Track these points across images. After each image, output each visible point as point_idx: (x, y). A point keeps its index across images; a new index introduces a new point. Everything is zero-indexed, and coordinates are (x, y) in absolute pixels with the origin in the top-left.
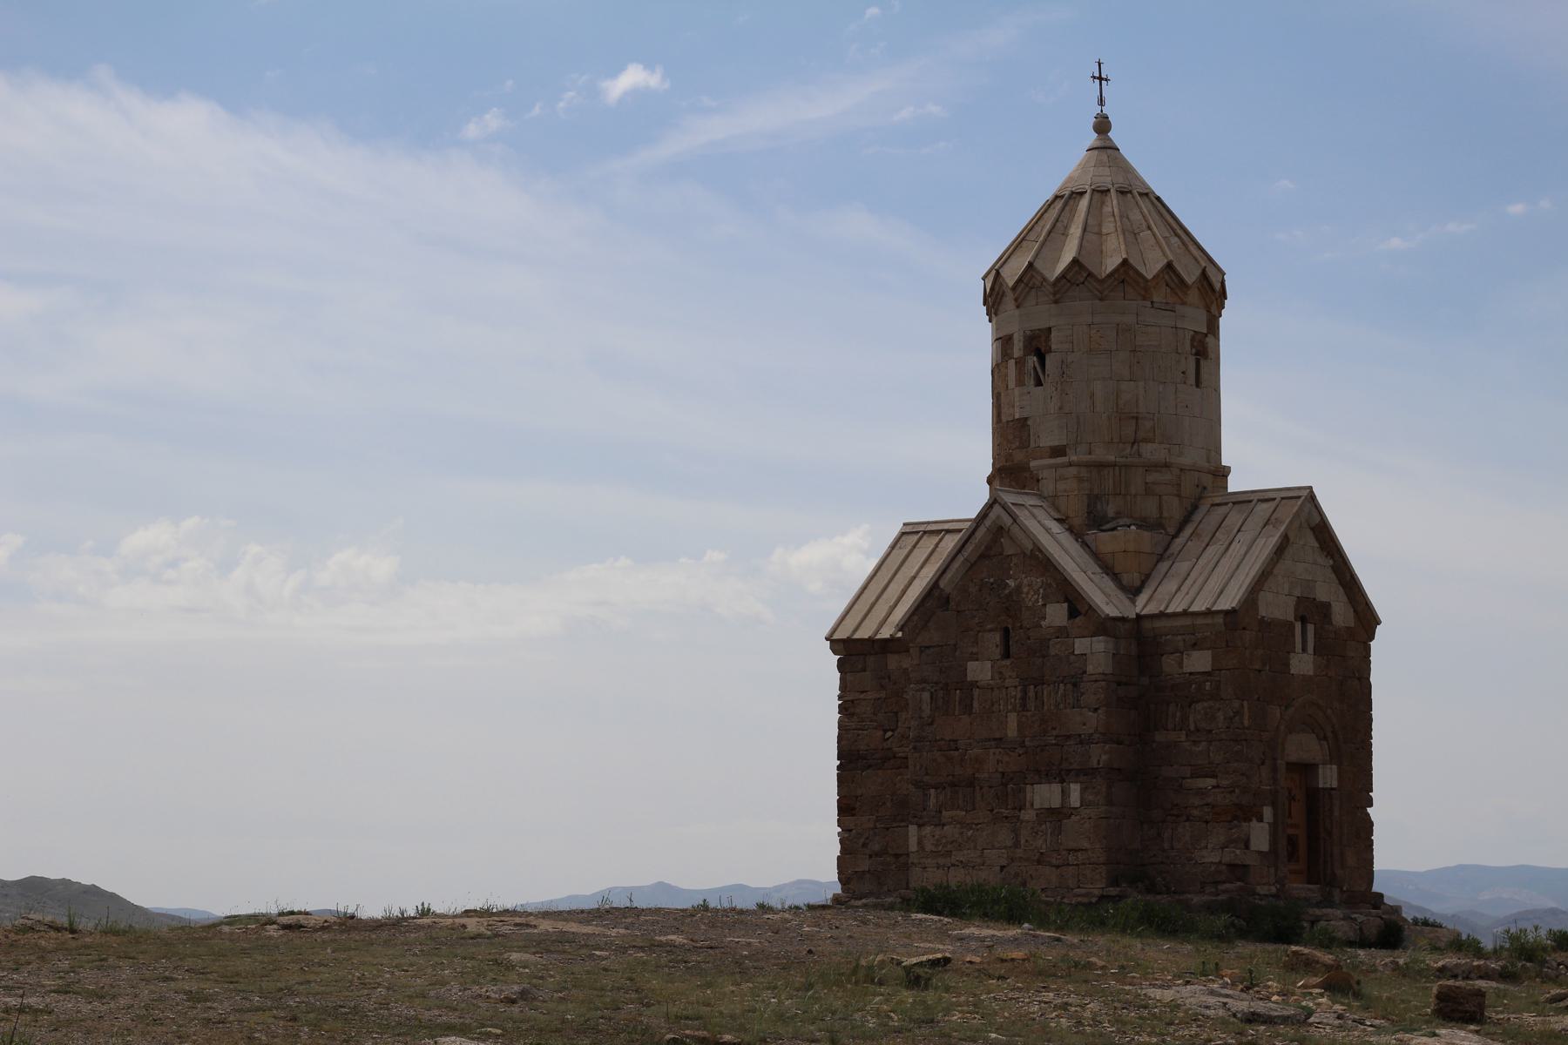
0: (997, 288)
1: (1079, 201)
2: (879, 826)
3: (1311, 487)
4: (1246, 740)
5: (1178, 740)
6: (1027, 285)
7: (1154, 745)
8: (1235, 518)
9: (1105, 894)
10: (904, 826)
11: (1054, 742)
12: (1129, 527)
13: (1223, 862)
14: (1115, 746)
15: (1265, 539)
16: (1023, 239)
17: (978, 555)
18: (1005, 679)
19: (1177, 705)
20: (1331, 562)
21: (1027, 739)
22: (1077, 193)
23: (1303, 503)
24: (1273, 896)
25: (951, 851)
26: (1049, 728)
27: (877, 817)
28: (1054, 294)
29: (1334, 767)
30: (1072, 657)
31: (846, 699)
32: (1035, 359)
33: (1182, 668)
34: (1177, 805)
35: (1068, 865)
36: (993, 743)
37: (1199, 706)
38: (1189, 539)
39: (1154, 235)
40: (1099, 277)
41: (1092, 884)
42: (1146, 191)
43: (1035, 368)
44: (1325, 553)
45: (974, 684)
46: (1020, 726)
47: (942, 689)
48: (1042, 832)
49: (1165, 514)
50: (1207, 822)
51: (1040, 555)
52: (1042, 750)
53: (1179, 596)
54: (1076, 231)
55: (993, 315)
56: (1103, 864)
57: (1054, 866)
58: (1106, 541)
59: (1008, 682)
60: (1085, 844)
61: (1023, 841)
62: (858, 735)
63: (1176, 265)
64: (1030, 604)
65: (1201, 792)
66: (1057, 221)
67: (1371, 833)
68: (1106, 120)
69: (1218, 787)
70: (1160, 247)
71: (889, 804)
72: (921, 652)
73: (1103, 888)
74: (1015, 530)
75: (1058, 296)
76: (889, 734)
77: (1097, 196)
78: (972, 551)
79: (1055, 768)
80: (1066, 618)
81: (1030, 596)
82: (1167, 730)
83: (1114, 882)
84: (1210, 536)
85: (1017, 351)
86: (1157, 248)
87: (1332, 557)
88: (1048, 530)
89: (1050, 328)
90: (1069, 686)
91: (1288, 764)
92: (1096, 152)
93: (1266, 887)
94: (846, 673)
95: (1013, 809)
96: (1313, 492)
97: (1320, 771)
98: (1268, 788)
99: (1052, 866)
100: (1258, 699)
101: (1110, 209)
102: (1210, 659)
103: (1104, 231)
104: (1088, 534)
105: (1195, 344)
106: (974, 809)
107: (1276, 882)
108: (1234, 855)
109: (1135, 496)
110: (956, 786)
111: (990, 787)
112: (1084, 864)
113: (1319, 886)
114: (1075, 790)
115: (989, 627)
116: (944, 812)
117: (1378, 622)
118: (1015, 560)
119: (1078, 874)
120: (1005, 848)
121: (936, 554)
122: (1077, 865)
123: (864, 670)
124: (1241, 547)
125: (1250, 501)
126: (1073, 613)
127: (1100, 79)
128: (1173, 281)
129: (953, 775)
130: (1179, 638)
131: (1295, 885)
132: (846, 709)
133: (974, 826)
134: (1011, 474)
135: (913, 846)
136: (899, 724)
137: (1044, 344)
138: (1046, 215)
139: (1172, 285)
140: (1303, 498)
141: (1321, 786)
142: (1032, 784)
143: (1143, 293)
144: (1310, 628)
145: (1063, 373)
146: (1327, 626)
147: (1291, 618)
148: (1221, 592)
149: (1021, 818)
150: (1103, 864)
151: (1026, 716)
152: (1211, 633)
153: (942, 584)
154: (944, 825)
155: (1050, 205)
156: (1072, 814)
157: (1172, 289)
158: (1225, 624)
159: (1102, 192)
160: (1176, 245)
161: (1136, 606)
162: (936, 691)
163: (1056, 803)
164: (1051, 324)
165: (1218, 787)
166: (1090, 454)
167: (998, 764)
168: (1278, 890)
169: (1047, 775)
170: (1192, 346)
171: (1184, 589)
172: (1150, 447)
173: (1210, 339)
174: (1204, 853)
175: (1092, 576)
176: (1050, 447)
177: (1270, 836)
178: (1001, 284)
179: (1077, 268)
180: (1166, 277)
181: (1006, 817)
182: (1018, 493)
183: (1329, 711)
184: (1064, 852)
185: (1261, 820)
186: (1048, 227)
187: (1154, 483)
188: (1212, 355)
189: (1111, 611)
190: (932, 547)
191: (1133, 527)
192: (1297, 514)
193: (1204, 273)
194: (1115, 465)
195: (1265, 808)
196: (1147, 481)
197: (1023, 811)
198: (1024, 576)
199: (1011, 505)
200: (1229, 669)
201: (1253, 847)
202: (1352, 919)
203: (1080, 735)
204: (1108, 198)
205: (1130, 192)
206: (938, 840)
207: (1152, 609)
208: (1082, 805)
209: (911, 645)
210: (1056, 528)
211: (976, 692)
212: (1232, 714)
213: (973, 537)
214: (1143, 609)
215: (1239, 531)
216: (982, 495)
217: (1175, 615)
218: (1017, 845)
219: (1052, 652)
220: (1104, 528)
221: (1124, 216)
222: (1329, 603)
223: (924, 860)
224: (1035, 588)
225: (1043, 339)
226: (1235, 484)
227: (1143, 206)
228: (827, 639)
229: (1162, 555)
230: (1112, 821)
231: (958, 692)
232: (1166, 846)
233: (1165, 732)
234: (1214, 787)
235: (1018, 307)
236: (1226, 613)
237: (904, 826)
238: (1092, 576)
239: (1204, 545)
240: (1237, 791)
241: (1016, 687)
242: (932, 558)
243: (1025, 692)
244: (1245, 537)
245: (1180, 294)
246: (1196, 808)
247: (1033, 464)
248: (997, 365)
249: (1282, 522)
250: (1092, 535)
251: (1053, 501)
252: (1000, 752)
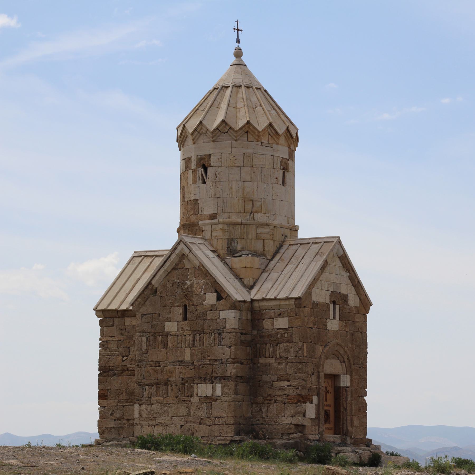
0: (183, 133)
1: (226, 91)
2: (119, 405)
3: (339, 237)
4: (304, 362)
5: (271, 362)
6: (199, 132)
7: (259, 365)
8: (301, 251)
9: (233, 439)
10: (132, 405)
11: (209, 363)
12: (248, 255)
13: (293, 423)
14: (239, 365)
15: (315, 262)
16: (197, 109)
17: (172, 267)
18: (184, 331)
19: (271, 345)
20: (348, 274)
21: (195, 361)
22: (225, 87)
23: (334, 244)
24: (317, 440)
25: (156, 418)
26: (206, 356)
27: (118, 400)
28: (213, 137)
29: (349, 376)
30: (218, 320)
31: (103, 340)
32: (202, 170)
33: (273, 326)
34: (270, 395)
35: (215, 425)
36: (178, 363)
37: (281, 345)
38: (278, 261)
39: (263, 109)
40: (235, 130)
41: (227, 434)
42: (260, 87)
43: (202, 174)
44: (345, 270)
45: (169, 334)
46: (192, 355)
47: (152, 336)
48: (202, 408)
49: (266, 249)
50: (285, 403)
51: (203, 269)
52: (203, 367)
53: (273, 290)
54: (224, 106)
55: (182, 147)
56: (233, 424)
57: (208, 425)
58: (236, 262)
59: (186, 333)
60: (224, 415)
61: (192, 413)
62: (110, 359)
63: (274, 124)
64: (198, 293)
65: (282, 388)
66: (215, 101)
67: (366, 409)
68: (240, 50)
69: (290, 386)
70: (266, 115)
71: (124, 394)
72: (142, 317)
73: (232, 436)
74: (191, 256)
75: (214, 138)
76: (125, 358)
77: (235, 88)
78: (168, 266)
79: (209, 376)
80: (216, 301)
81: (197, 289)
82: (266, 357)
83: (238, 433)
84: (289, 260)
85: (193, 165)
86: (264, 116)
87: (349, 272)
88: (207, 256)
89: (210, 155)
90: (217, 335)
91: (325, 374)
92: (235, 67)
93: (314, 436)
94: (103, 327)
95: (187, 396)
96: (339, 239)
97: (341, 378)
98: (316, 386)
99: (207, 425)
100: (311, 342)
101: (241, 96)
102: (287, 322)
103: (238, 106)
104: (227, 258)
105: (283, 164)
106: (168, 396)
107: (319, 433)
108: (298, 420)
109: (251, 239)
110: (158, 384)
111: (176, 385)
112: (222, 424)
113: (340, 435)
114: (219, 387)
115: (177, 304)
116: (152, 398)
117: (371, 305)
118: (190, 271)
119: (220, 429)
120: (183, 416)
121: (150, 267)
122: (219, 425)
123: (113, 326)
124: (303, 267)
125: (309, 243)
126: (219, 298)
127: (238, 30)
128: (272, 133)
129: (157, 379)
130: (272, 311)
131: (328, 435)
132: (103, 345)
133: (167, 405)
134: (189, 227)
135: (136, 415)
136: (131, 353)
137: (207, 162)
138: (209, 98)
139: (272, 134)
140: (335, 242)
141: (341, 385)
142: (197, 384)
143: (257, 138)
144: (338, 307)
145: (216, 177)
146: (345, 306)
147: (328, 302)
148: (294, 288)
149: (191, 401)
150: (233, 424)
151: (195, 350)
152: (288, 309)
153: (153, 282)
154: (152, 404)
155: (211, 93)
156: (217, 399)
157: (271, 136)
158: (295, 304)
159: (237, 87)
160: (274, 114)
161: (250, 295)
162: (149, 336)
163: (209, 394)
164: (211, 153)
165: (290, 386)
166: (229, 218)
167: (180, 374)
168: (320, 438)
169: (205, 379)
170: (281, 165)
171: (275, 287)
172: (259, 215)
173: (290, 162)
174: (283, 419)
175: (229, 280)
176: (210, 215)
177: (316, 410)
178: (186, 132)
179: (224, 124)
180: (269, 130)
181: (184, 401)
182: (193, 237)
183: (346, 348)
184: (213, 418)
185: (311, 402)
186: (210, 103)
187: (260, 233)
188: (290, 170)
189: (240, 298)
190: (149, 264)
191: (250, 255)
192: (332, 250)
193: (288, 129)
194: (242, 224)
195: (314, 396)
196: (257, 232)
197: (192, 398)
198: (195, 279)
199: (189, 243)
200: (297, 327)
201: (308, 415)
202: (356, 452)
203: (222, 360)
204: (240, 90)
205: (252, 87)
206: (149, 412)
207: (259, 297)
208: (222, 395)
209: (137, 313)
210: (211, 255)
211: (170, 337)
212: (298, 349)
213: (169, 259)
214: (254, 296)
215: (303, 258)
216: (174, 238)
217: (270, 300)
218: (189, 415)
219: (208, 317)
220: (236, 255)
221: (248, 99)
222: (347, 294)
223: (142, 422)
224: (201, 285)
225: (206, 160)
226: (301, 235)
227: (258, 95)
228: (94, 310)
229: (264, 269)
230: (237, 402)
231: (160, 337)
232: (264, 415)
233: (264, 358)
234: (288, 386)
235: (194, 143)
236: (296, 299)
237: (132, 405)
238: (229, 280)
239: (285, 265)
240: (300, 388)
241: (190, 335)
242: (149, 269)
243: (194, 337)
244: (305, 261)
245: (276, 139)
246: (279, 396)
247: (200, 223)
248: (183, 172)
249: (324, 254)
250: (229, 259)
251: (210, 241)
252: (181, 368)
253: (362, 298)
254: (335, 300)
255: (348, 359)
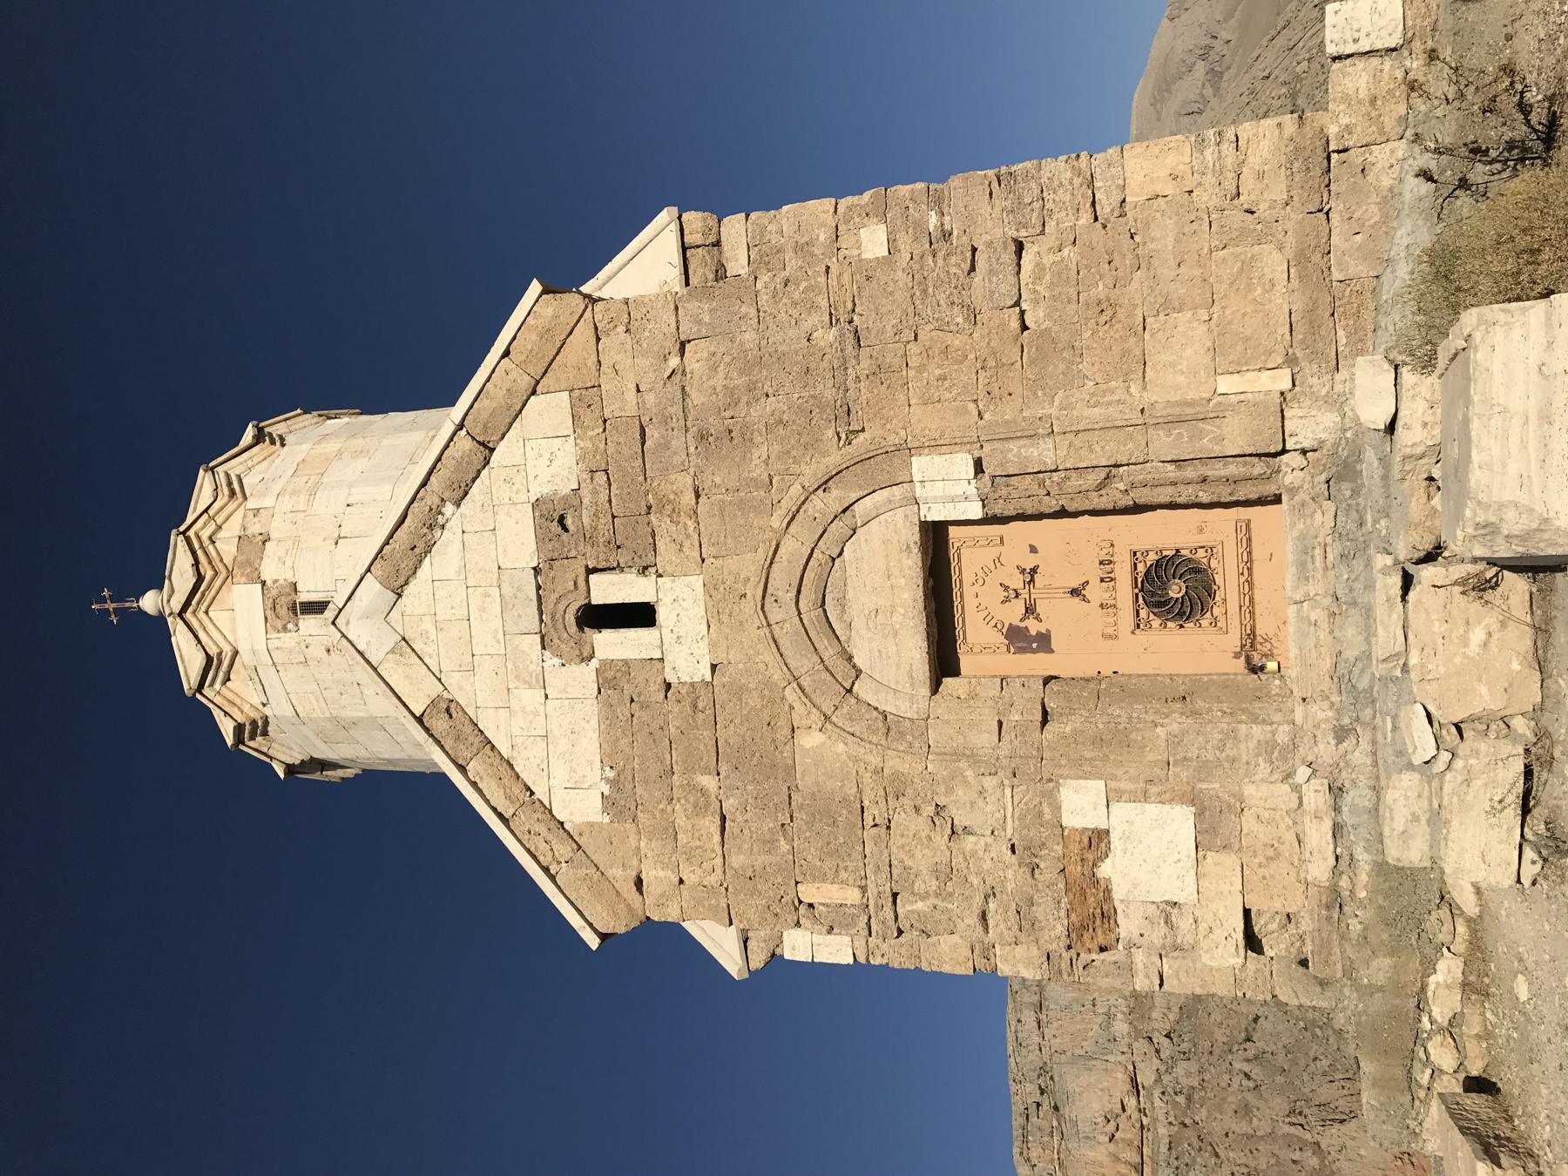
20: (449, 509)
147: (588, 671)
180: (217, 686)
253: (525, 382)
254: (571, 619)
255: (824, 486)
